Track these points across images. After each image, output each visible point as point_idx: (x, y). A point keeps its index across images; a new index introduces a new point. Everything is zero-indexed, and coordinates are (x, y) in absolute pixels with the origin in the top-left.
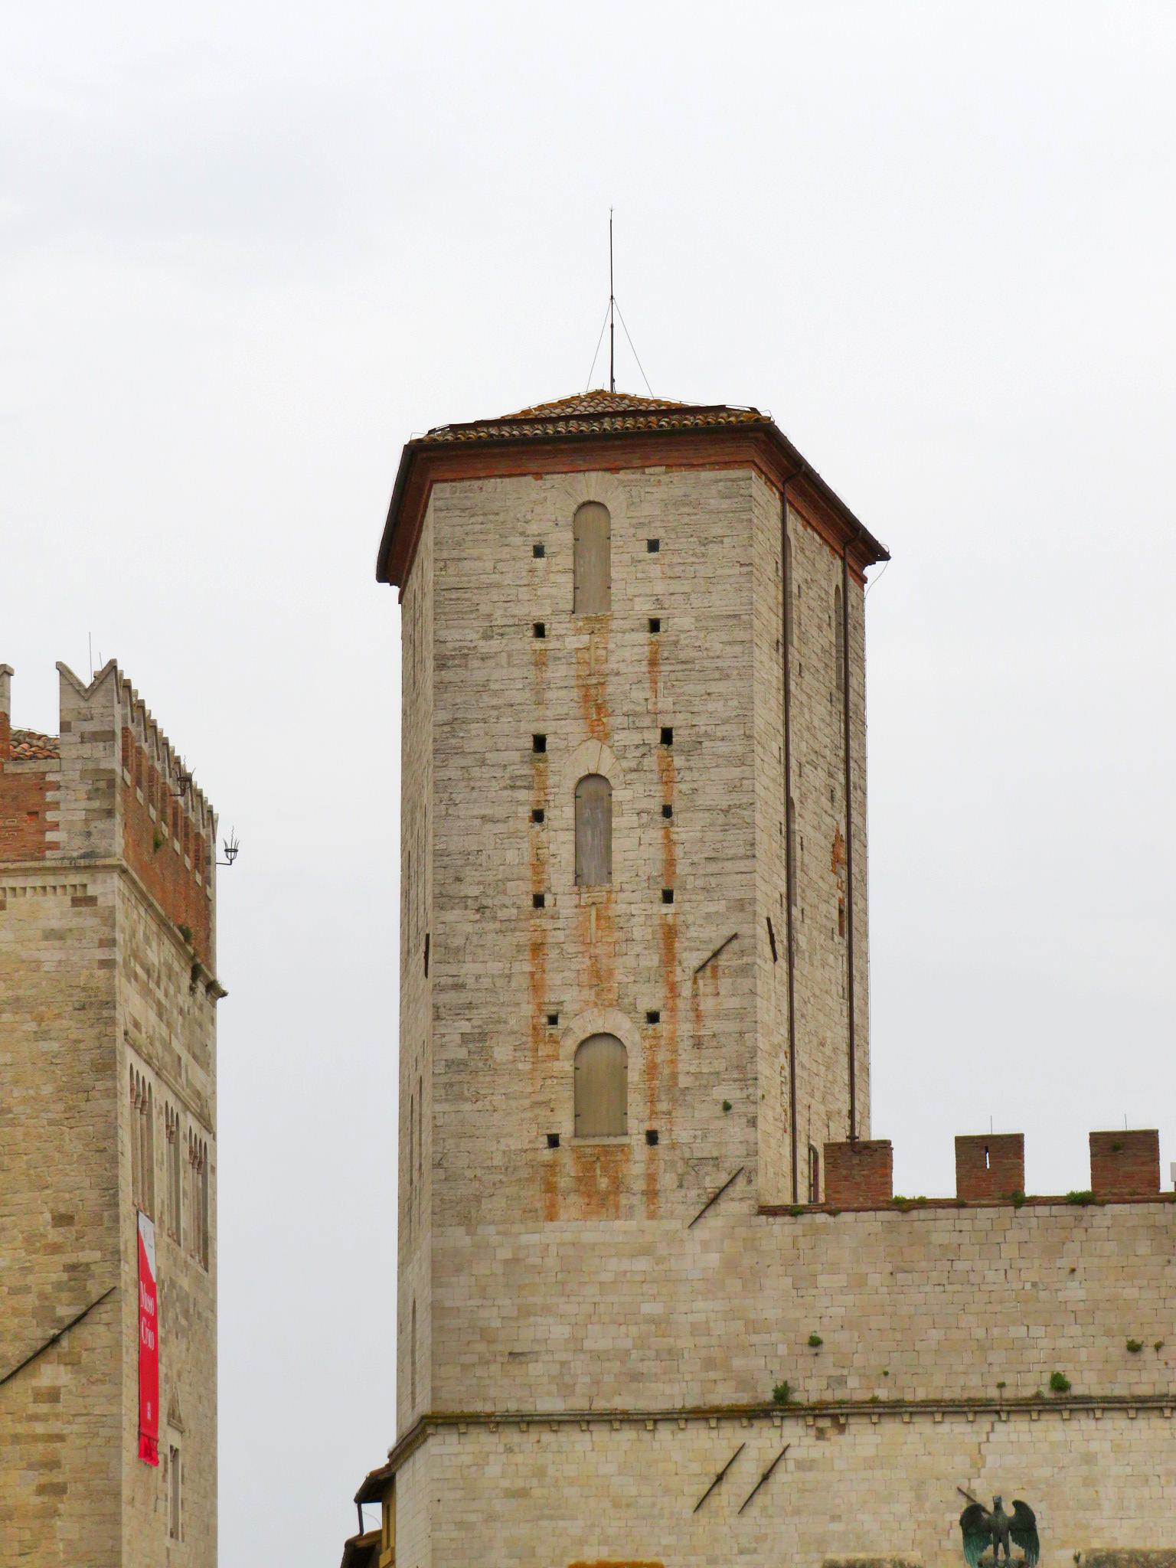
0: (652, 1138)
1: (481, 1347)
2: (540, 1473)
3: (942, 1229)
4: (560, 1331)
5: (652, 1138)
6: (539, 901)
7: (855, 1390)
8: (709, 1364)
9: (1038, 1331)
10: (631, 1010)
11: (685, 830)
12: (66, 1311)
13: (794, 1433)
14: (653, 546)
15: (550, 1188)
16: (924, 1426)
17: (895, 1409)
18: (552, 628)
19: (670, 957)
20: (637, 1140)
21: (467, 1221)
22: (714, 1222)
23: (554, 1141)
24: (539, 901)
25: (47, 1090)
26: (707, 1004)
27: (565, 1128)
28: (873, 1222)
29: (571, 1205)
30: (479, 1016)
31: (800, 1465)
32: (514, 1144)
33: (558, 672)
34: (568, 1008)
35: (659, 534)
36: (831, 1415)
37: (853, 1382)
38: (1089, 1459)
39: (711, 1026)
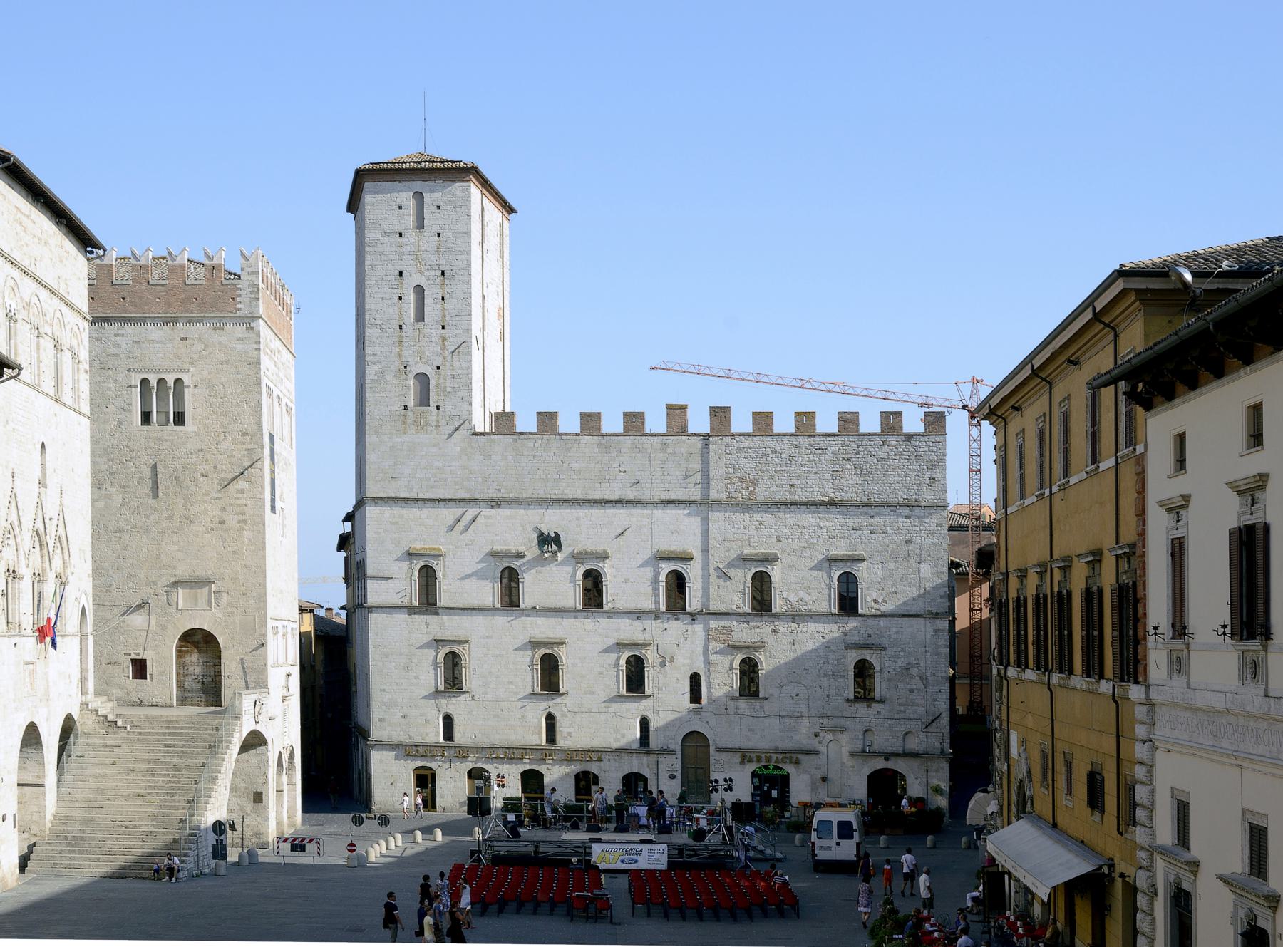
0: (438, 408)
4: (408, 471)
5: (438, 408)
7: (504, 494)
12: (246, 464)
15: (404, 423)
17: (516, 501)
23: (405, 408)
25: (239, 391)
27: (411, 403)
28: (509, 439)
29: (412, 429)
31: (486, 517)
34: (412, 363)
36: (495, 503)
38: (578, 519)
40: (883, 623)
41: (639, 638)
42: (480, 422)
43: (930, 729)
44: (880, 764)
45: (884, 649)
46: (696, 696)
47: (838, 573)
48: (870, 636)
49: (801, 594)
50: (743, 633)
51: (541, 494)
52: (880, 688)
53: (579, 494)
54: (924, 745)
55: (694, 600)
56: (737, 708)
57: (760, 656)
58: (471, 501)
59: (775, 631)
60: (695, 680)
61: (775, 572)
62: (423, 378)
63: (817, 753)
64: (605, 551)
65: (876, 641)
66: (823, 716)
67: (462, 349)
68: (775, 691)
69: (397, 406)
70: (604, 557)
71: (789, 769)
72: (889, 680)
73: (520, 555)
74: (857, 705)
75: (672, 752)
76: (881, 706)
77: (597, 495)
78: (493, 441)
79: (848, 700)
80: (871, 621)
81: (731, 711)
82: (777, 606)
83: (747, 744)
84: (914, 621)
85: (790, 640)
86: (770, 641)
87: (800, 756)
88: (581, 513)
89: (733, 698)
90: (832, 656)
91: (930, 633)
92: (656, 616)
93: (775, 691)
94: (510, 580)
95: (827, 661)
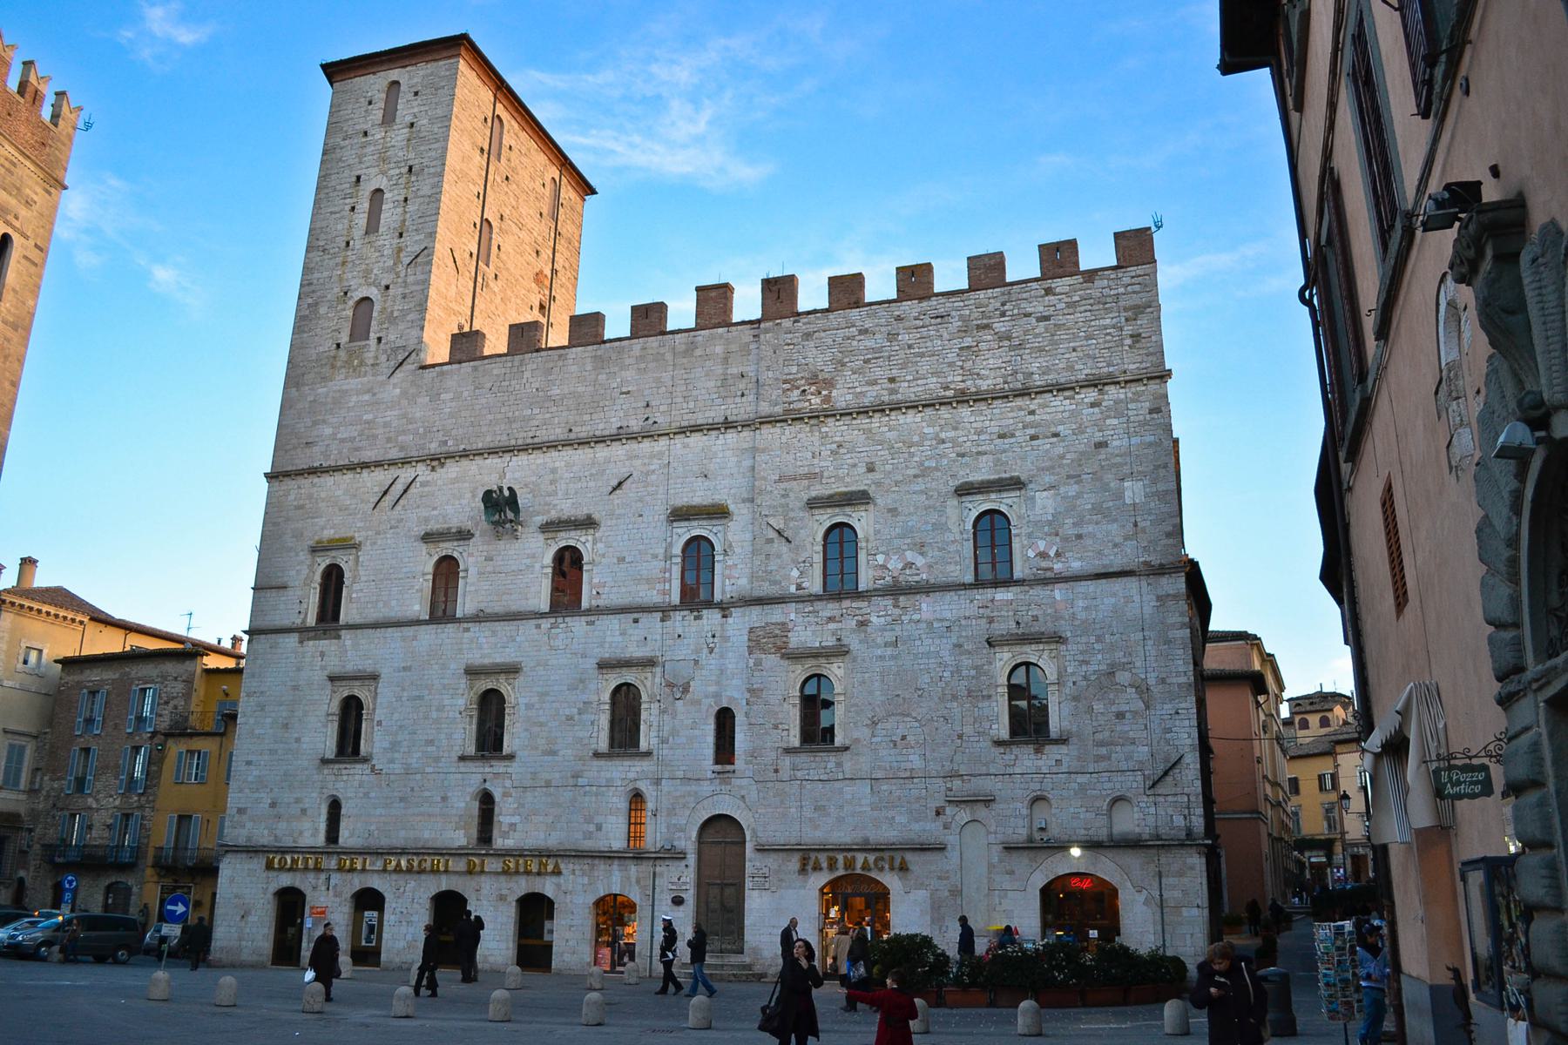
0: (379, 339)
1: (295, 441)
2: (310, 497)
3: (497, 369)
4: (328, 431)
5: (379, 339)
7: (451, 446)
8: (389, 440)
9: (536, 411)
10: (375, 284)
11: (411, 208)
13: (421, 468)
14: (416, 94)
15: (333, 367)
16: (479, 460)
17: (465, 455)
18: (371, 132)
19: (397, 261)
20: (373, 342)
21: (298, 385)
22: (399, 375)
23: (338, 345)
26: (410, 279)
27: (344, 338)
30: (315, 296)
31: (423, 484)
36: (437, 460)
37: (450, 443)
38: (554, 471)
40: (1058, 593)
43: (1160, 789)
45: (1059, 639)
46: (724, 749)
48: (1036, 619)
49: (910, 556)
50: (806, 631)
51: (503, 440)
53: (558, 433)
54: (1151, 820)
55: (730, 578)
57: (835, 670)
58: (405, 462)
59: (863, 624)
60: (725, 720)
61: (862, 521)
63: (941, 848)
64: (589, 517)
65: (1049, 627)
67: (423, 258)
69: (329, 345)
70: (589, 523)
71: (890, 880)
72: (1076, 699)
73: (464, 535)
74: (1016, 750)
76: (1064, 749)
77: (582, 432)
78: (442, 373)
79: (999, 743)
80: (1038, 592)
81: (785, 774)
84: (1117, 585)
85: (889, 636)
88: (558, 459)
89: (788, 751)
90: (966, 661)
91: (1150, 604)
92: (665, 611)
93: (863, 733)
94: (447, 571)
95: (957, 671)
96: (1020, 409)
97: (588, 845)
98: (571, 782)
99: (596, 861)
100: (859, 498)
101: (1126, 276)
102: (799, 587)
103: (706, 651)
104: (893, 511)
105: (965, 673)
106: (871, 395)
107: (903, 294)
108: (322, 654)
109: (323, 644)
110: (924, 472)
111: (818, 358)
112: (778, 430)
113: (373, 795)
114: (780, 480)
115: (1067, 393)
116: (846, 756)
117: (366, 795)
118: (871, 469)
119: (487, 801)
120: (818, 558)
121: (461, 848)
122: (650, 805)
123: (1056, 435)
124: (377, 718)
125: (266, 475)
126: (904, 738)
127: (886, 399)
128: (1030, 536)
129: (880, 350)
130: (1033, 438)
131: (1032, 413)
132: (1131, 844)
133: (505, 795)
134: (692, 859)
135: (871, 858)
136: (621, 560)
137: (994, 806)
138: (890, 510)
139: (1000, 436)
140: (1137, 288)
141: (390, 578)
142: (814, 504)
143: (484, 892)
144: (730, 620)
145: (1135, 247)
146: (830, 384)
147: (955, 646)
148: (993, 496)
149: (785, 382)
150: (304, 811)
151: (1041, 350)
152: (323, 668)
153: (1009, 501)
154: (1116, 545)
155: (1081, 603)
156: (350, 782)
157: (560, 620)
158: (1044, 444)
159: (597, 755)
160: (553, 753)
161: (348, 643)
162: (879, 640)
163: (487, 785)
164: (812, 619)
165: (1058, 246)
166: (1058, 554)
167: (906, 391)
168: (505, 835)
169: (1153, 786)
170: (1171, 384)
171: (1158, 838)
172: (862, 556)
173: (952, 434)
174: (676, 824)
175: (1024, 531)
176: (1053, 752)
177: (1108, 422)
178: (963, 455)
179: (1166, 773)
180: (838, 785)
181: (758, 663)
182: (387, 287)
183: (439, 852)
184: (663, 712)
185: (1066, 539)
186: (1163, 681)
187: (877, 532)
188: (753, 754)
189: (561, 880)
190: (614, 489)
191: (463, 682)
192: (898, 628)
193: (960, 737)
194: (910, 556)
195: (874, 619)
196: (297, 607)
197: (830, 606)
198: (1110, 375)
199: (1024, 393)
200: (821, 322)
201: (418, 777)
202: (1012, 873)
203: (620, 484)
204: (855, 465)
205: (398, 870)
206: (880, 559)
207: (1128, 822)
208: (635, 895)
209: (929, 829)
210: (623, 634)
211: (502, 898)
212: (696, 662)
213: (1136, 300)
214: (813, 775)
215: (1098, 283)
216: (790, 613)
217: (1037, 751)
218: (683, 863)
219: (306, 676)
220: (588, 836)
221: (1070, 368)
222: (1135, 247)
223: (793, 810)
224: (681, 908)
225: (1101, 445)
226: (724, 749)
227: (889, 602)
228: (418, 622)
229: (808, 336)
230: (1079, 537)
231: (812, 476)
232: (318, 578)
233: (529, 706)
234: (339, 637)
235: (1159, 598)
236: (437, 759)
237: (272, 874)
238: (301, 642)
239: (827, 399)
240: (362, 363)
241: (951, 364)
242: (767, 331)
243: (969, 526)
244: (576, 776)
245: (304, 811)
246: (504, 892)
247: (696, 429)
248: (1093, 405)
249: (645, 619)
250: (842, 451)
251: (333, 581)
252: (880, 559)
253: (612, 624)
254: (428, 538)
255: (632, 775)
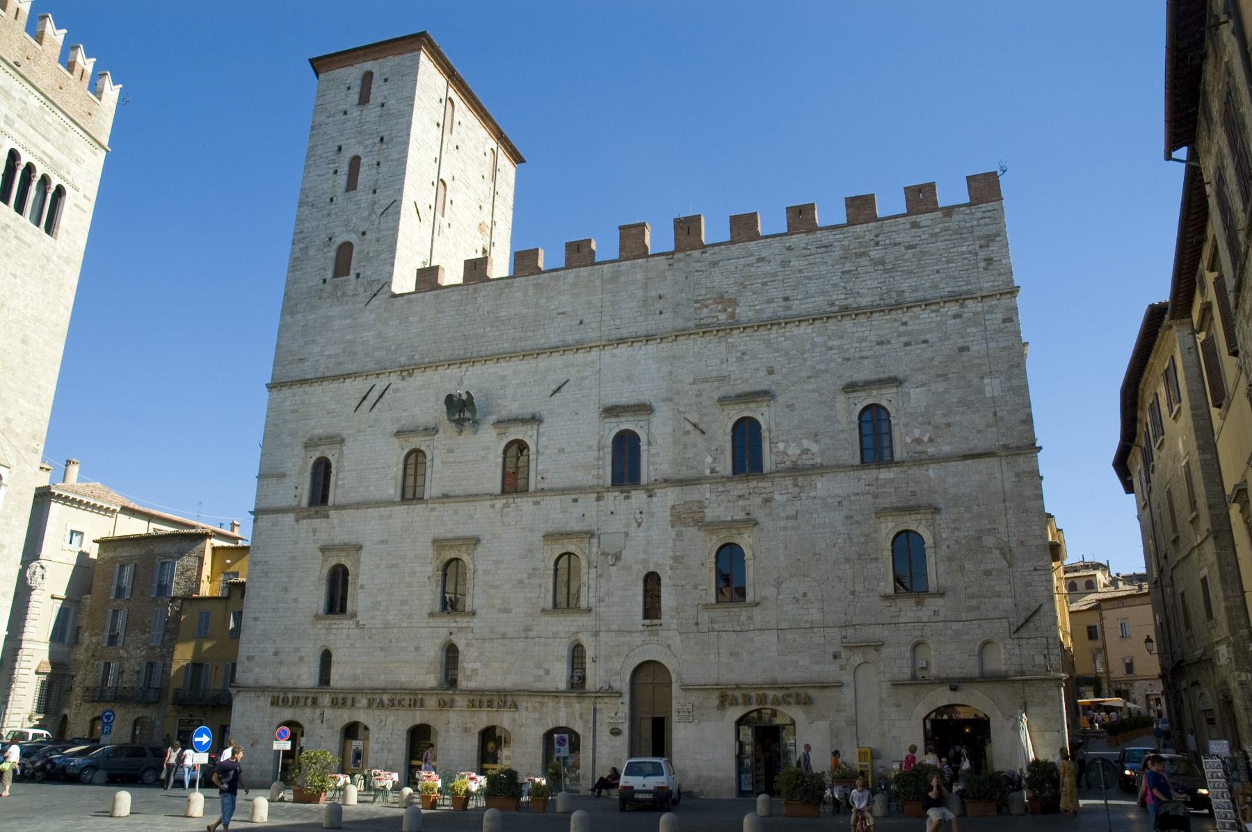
0: (358, 275)
3: (455, 297)
4: (317, 349)
5: (358, 275)
6: (332, 200)
8: (367, 355)
11: (383, 169)
21: (292, 313)
23: (325, 281)
24: (332, 200)
26: (382, 226)
27: (329, 274)
28: (430, 295)
32: (311, 284)
33: (349, 125)
35: (388, 76)
36: (407, 371)
37: (417, 357)
38: (504, 378)
39: (384, 233)
40: (933, 472)
41: (575, 526)
42: (403, 281)
43: (1023, 633)
44: (943, 697)
45: (937, 510)
46: (652, 609)
47: (859, 408)
48: (914, 494)
49: (806, 443)
52: (936, 572)
56: (712, 621)
57: (745, 541)
60: (652, 582)
61: (763, 415)
62: (346, 249)
63: (839, 685)
66: (845, 626)
68: (770, 591)
70: (535, 420)
72: (950, 559)
73: (431, 431)
74: (900, 603)
75: (620, 694)
76: (940, 601)
78: (410, 301)
79: (886, 597)
80: (915, 472)
81: (704, 627)
82: (768, 462)
83: (729, 677)
84: (982, 464)
85: (791, 510)
86: (760, 515)
87: (811, 692)
88: (506, 368)
89: (707, 607)
93: (770, 591)
94: (415, 458)
96: (895, 320)
97: (539, 686)
98: (523, 634)
99: (546, 700)
100: (764, 395)
101: (979, 211)
102: (713, 471)
103: (634, 525)
104: (790, 407)
105: (855, 540)
106: (769, 310)
107: (792, 229)
108: (314, 531)
109: (316, 522)
110: (816, 374)
111: (721, 281)
112: (691, 342)
113: (357, 645)
114: (694, 383)
115: (934, 307)
116: (756, 610)
117: (352, 645)
118: (771, 372)
119: (451, 653)
120: (729, 447)
121: (432, 689)
122: (589, 654)
123: (925, 342)
124: (360, 583)
125: (268, 386)
126: (805, 595)
127: (781, 314)
128: (906, 425)
129: (775, 274)
130: (906, 344)
131: (905, 324)
132: (999, 679)
133: (468, 645)
134: (626, 698)
135: (780, 694)
136: (562, 450)
137: (883, 650)
138: (788, 406)
139: (880, 343)
140: (988, 221)
141: (369, 466)
142: (724, 401)
143: (452, 725)
144: (655, 499)
145: (985, 188)
146: (734, 302)
147: (847, 517)
148: (875, 392)
149: (697, 302)
150: (301, 658)
151: (910, 272)
152: (316, 541)
153: (889, 397)
154: (979, 432)
155: (951, 480)
156: (339, 635)
157: (511, 501)
158: (917, 349)
159: (544, 611)
160: (508, 611)
161: (335, 521)
162: (782, 514)
163: (455, 639)
164: (723, 497)
165: (920, 189)
166: (931, 440)
167: (798, 307)
168: (469, 678)
169: (1018, 630)
170: (1020, 300)
171: (1023, 673)
172: (766, 445)
173: (836, 343)
174: (610, 668)
175: (903, 420)
176: (932, 604)
177: (969, 330)
178: (848, 359)
179: (1027, 621)
180: (749, 635)
181: (679, 535)
182: (364, 233)
183: (413, 691)
184: (599, 576)
185: (937, 427)
186: (1023, 543)
187: (777, 424)
188: (678, 610)
189: (517, 715)
190: (555, 392)
191: (430, 553)
192: (797, 503)
193: (853, 593)
194: (806, 443)
195: (777, 497)
196: (293, 492)
197: (740, 486)
198: (969, 291)
199: (896, 307)
200: (724, 252)
201: (396, 630)
202: (898, 705)
203: (559, 388)
204: (757, 369)
205: (381, 705)
206: (781, 446)
207: (999, 660)
208: (578, 728)
209: (830, 670)
210: (564, 511)
211: (466, 730)
212: (626, 534)
213: (986, 231)
214: (728, 626)
215: (955, 218)
216: (705, 492)
217: (918, 604)
218: (620, 700)
219: (303, 549)
220: (538, 679)
221: (935, 287)
222: (985, 188)
223: (712, 656)
224: (618, 738)
225: (963, 349)
226: (652, 609)
227: (789, 482)
228: (391, 503)
229: (714, 264)
230: (948, 425)
231: (721, 379)
232: (309, 468)
233: (486, 572)
234: (328, 517)
235: (1017, 475)
236: (410, 616)
237: (276, 710)
238: (297, 521)
239: (732, 315)
240: (344, 295)
241: (835, 285)
242: (680, 260)
243: (855, 418)
244: (527, 630)
245: (301, 658)
246: (469, 725)
247: (621, 341)
248: (955, 317)
249: (581, 497)
250: (746, 357)
251: (322, 471)
252: (781, 446)
253: (554, 504)
254: (399, 433)
255: (573, 629)
